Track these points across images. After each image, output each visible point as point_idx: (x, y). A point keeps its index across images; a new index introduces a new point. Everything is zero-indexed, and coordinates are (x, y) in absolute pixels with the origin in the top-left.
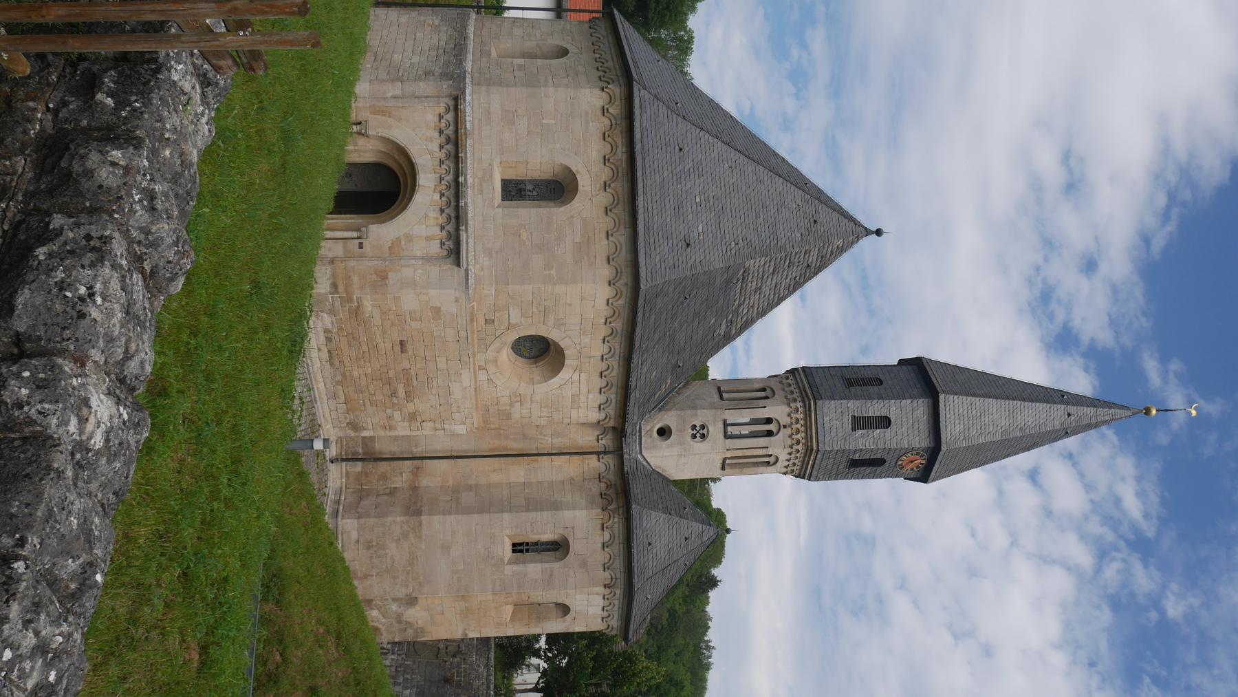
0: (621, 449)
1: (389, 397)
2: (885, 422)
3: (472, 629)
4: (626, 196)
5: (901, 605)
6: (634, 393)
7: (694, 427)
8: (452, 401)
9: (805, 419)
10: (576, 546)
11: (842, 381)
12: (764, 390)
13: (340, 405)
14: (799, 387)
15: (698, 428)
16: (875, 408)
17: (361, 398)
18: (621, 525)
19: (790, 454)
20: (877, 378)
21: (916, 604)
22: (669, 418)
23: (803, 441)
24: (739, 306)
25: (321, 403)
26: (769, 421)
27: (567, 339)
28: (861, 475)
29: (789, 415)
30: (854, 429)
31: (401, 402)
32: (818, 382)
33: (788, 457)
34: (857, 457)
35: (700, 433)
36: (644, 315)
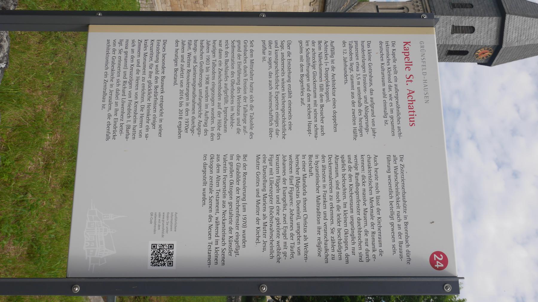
1: (194, 3)
2: (471, 30)
5: (469, 148)
6: (329, 5)
8: (228, 7)
11: (449, 5)
12: (403, 8)
13: (168, 7)
14: (423, 7)
16: (466, 21)
17: (179, 3)
20: (470, 4)
21: (478, 147)
25: (158, 6)
28: (453, 60)
30: (452, 33)
31: (201, 6)
32: (435, 4)
34: (452, 49)
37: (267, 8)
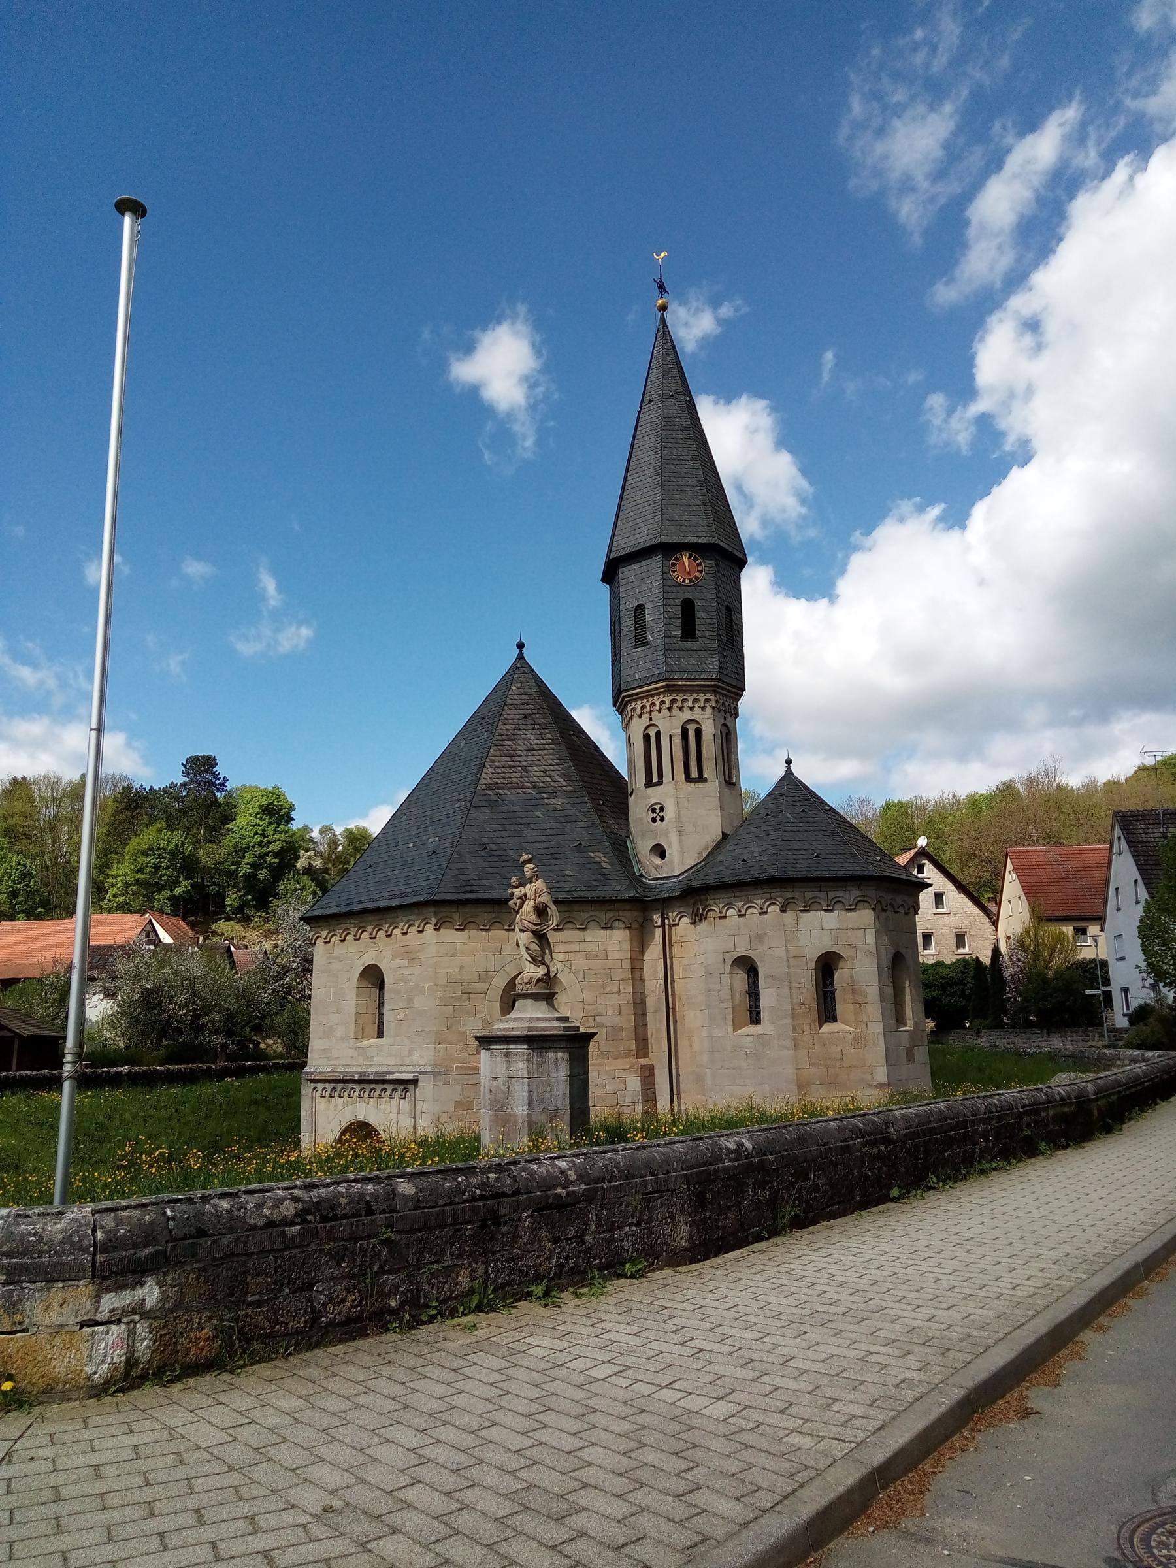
0: (658, 900)
2: (640, 609)
3: (869, 1077)
4: (377, 917)
7: (654, 820)
9: (641, 699)
10: (743, 949)
15: (655, 815)
18: (716, 897)
19: (681, 709)
22: (642, 846)
23: (662, 696)
24: (535, 787)
26: (647, 738)
27: (507, 968)
29: (640, 716)
30: (646, 644)
33: (686, 710)
35: (658, 812)
36: (470, 892)
37: (592, 1014)
